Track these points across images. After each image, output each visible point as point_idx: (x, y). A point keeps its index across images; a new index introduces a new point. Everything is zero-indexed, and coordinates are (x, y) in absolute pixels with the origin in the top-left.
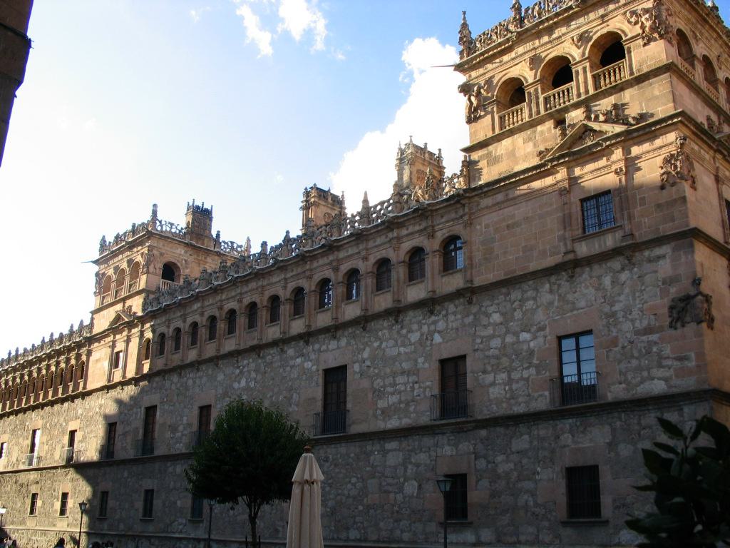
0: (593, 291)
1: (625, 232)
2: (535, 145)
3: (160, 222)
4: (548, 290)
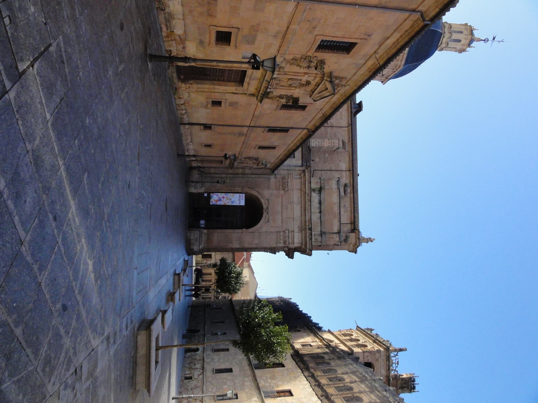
3: (397, 355)
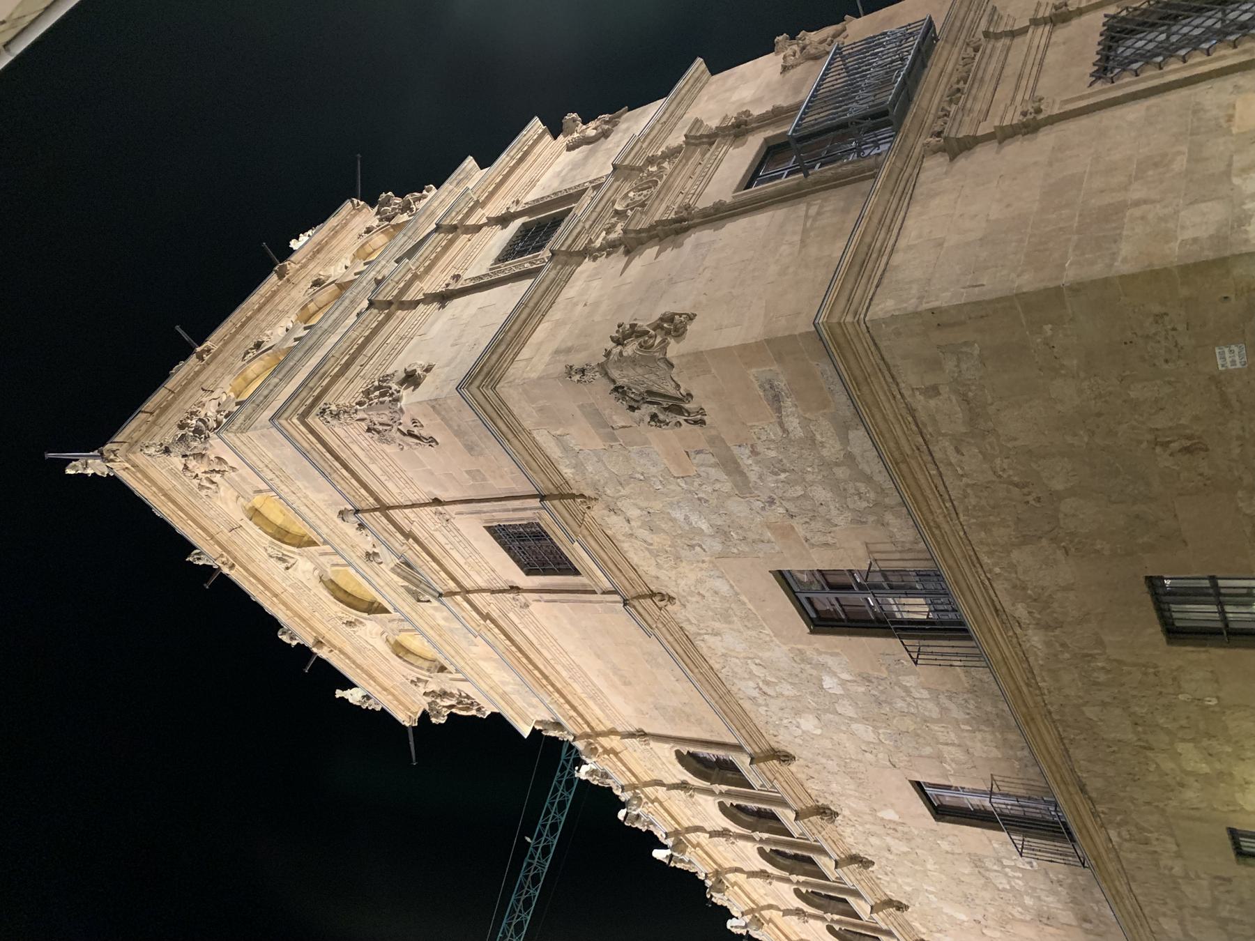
0: (684, 567)
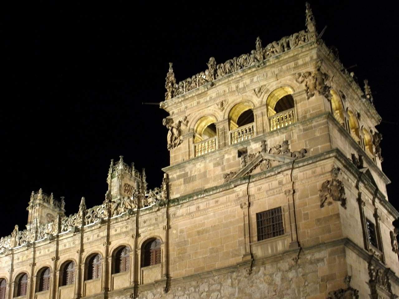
1: (292, 240)
2: (223, 169)
4: (230, 285)
